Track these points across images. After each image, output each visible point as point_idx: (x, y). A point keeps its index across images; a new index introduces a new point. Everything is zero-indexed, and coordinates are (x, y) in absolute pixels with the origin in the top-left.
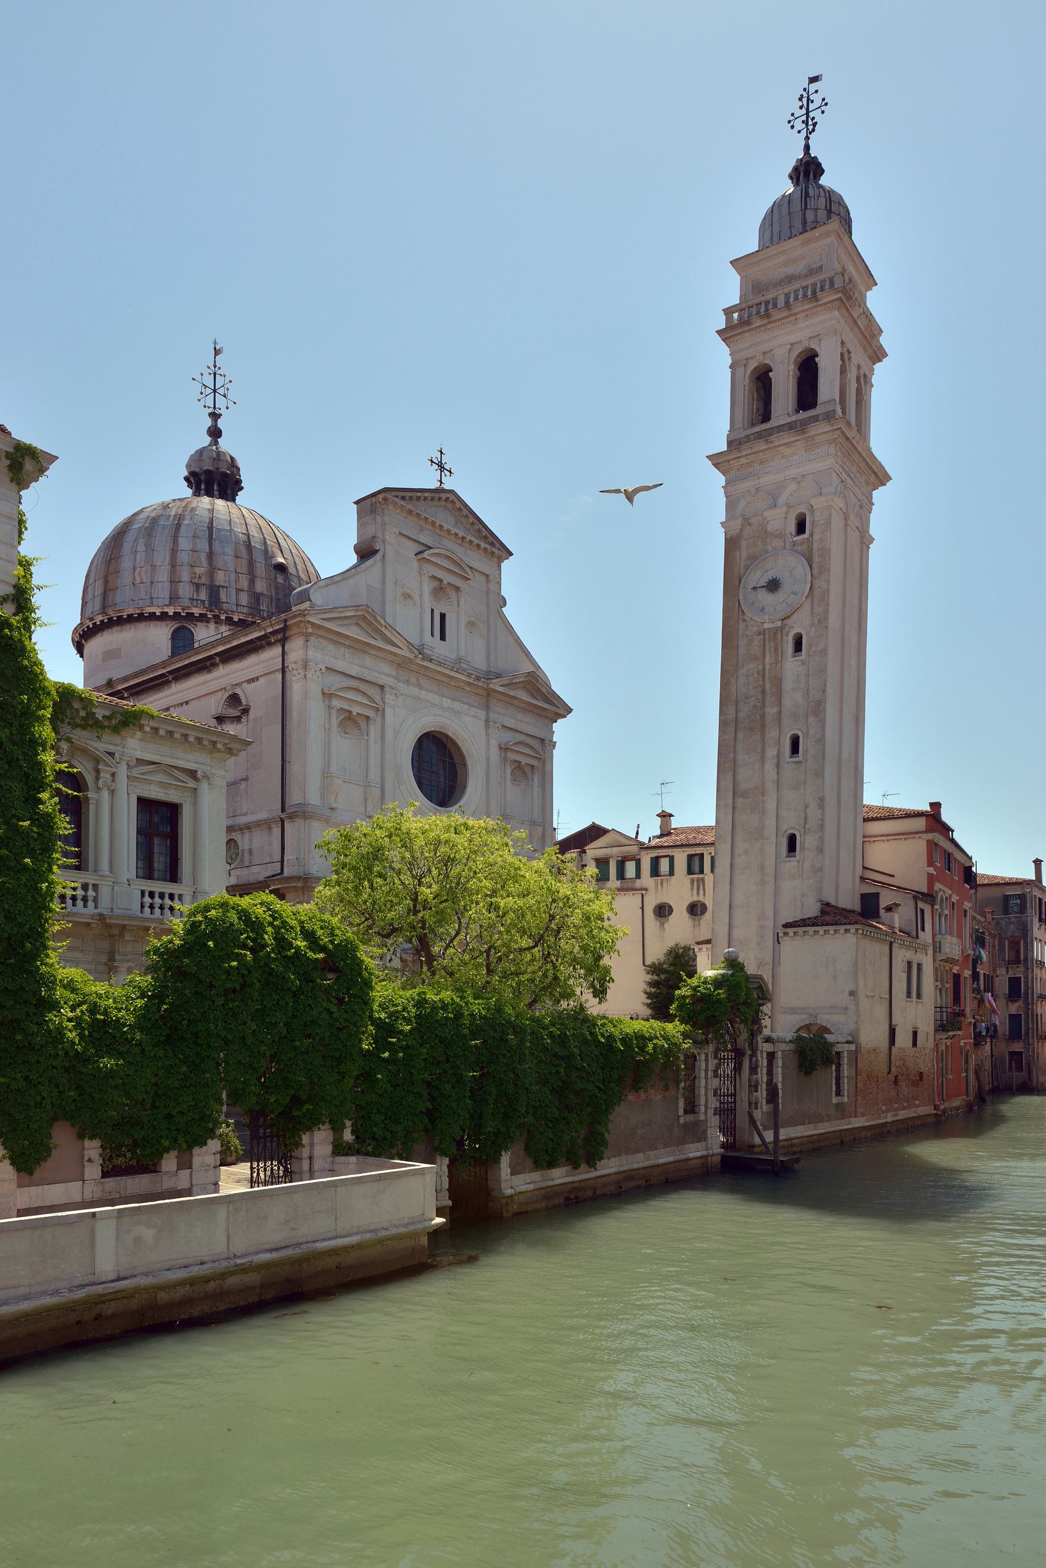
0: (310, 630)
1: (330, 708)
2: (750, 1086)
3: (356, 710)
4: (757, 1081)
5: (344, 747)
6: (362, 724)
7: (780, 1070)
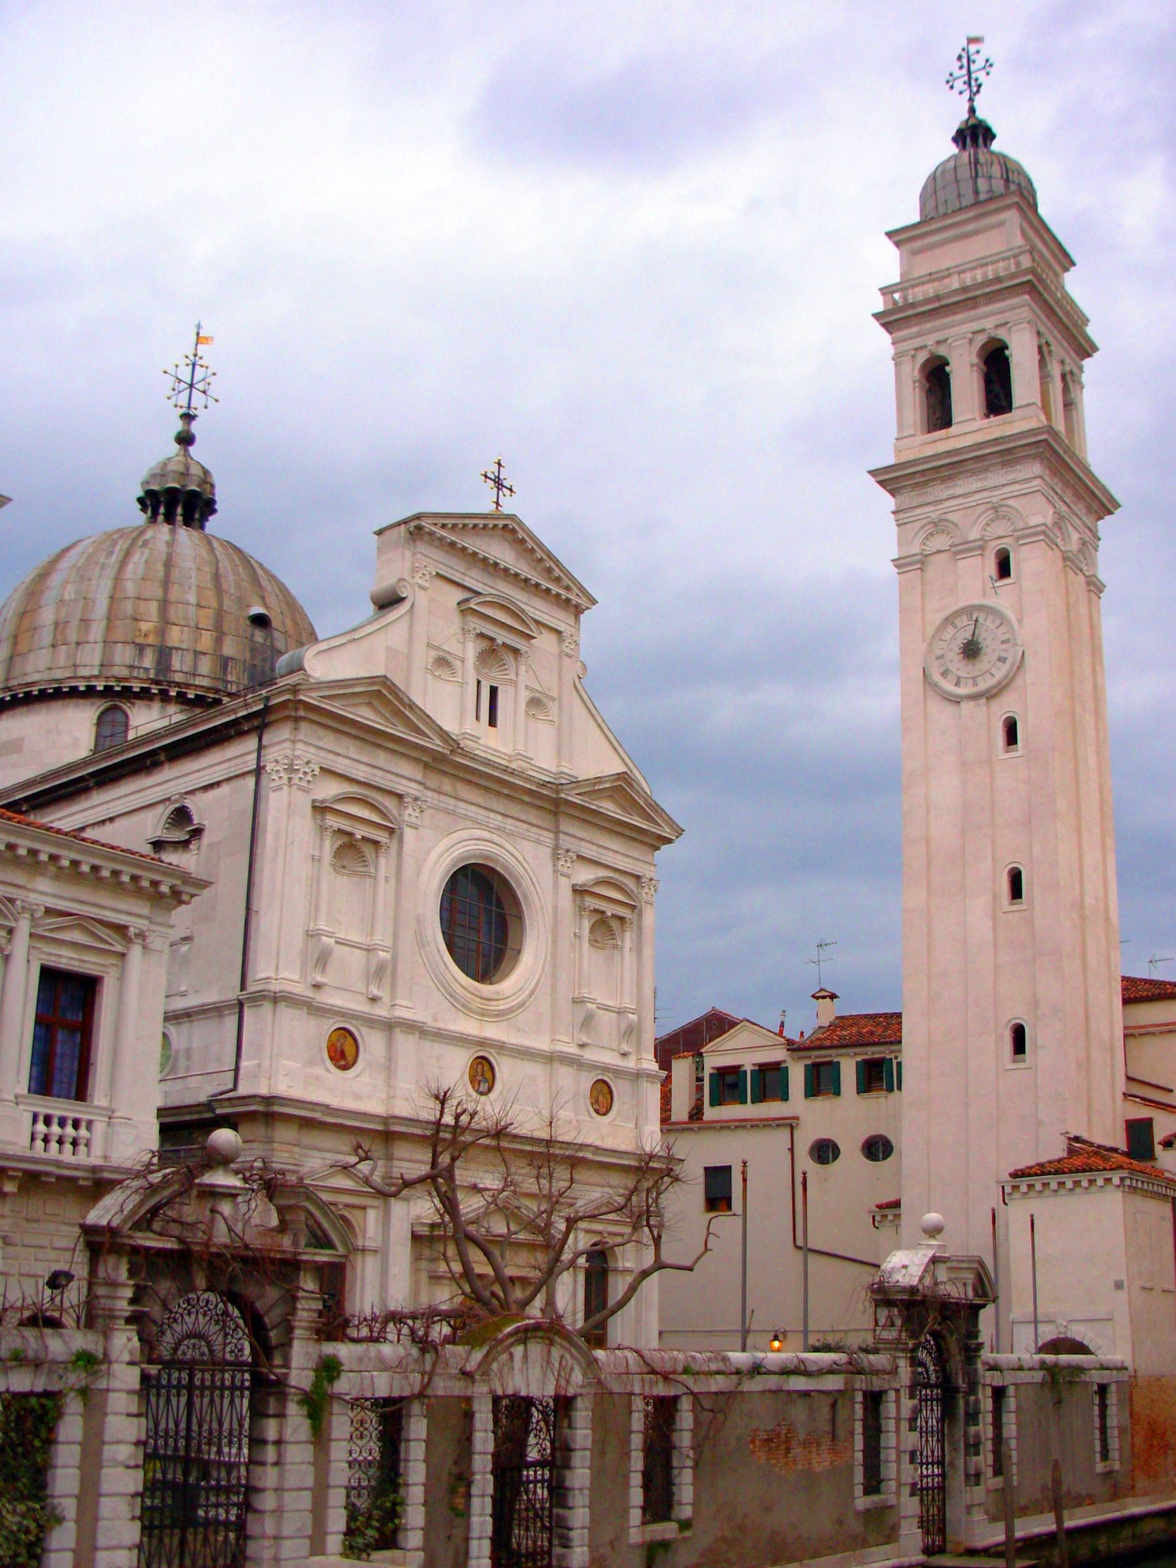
0: (302, 713)
1: (323, 829)
2: (967, 1445)
3: (360, 832)
4: (977, 1436)
5: (340, 889)
6: (368, 850)
7: (1013, 1416)
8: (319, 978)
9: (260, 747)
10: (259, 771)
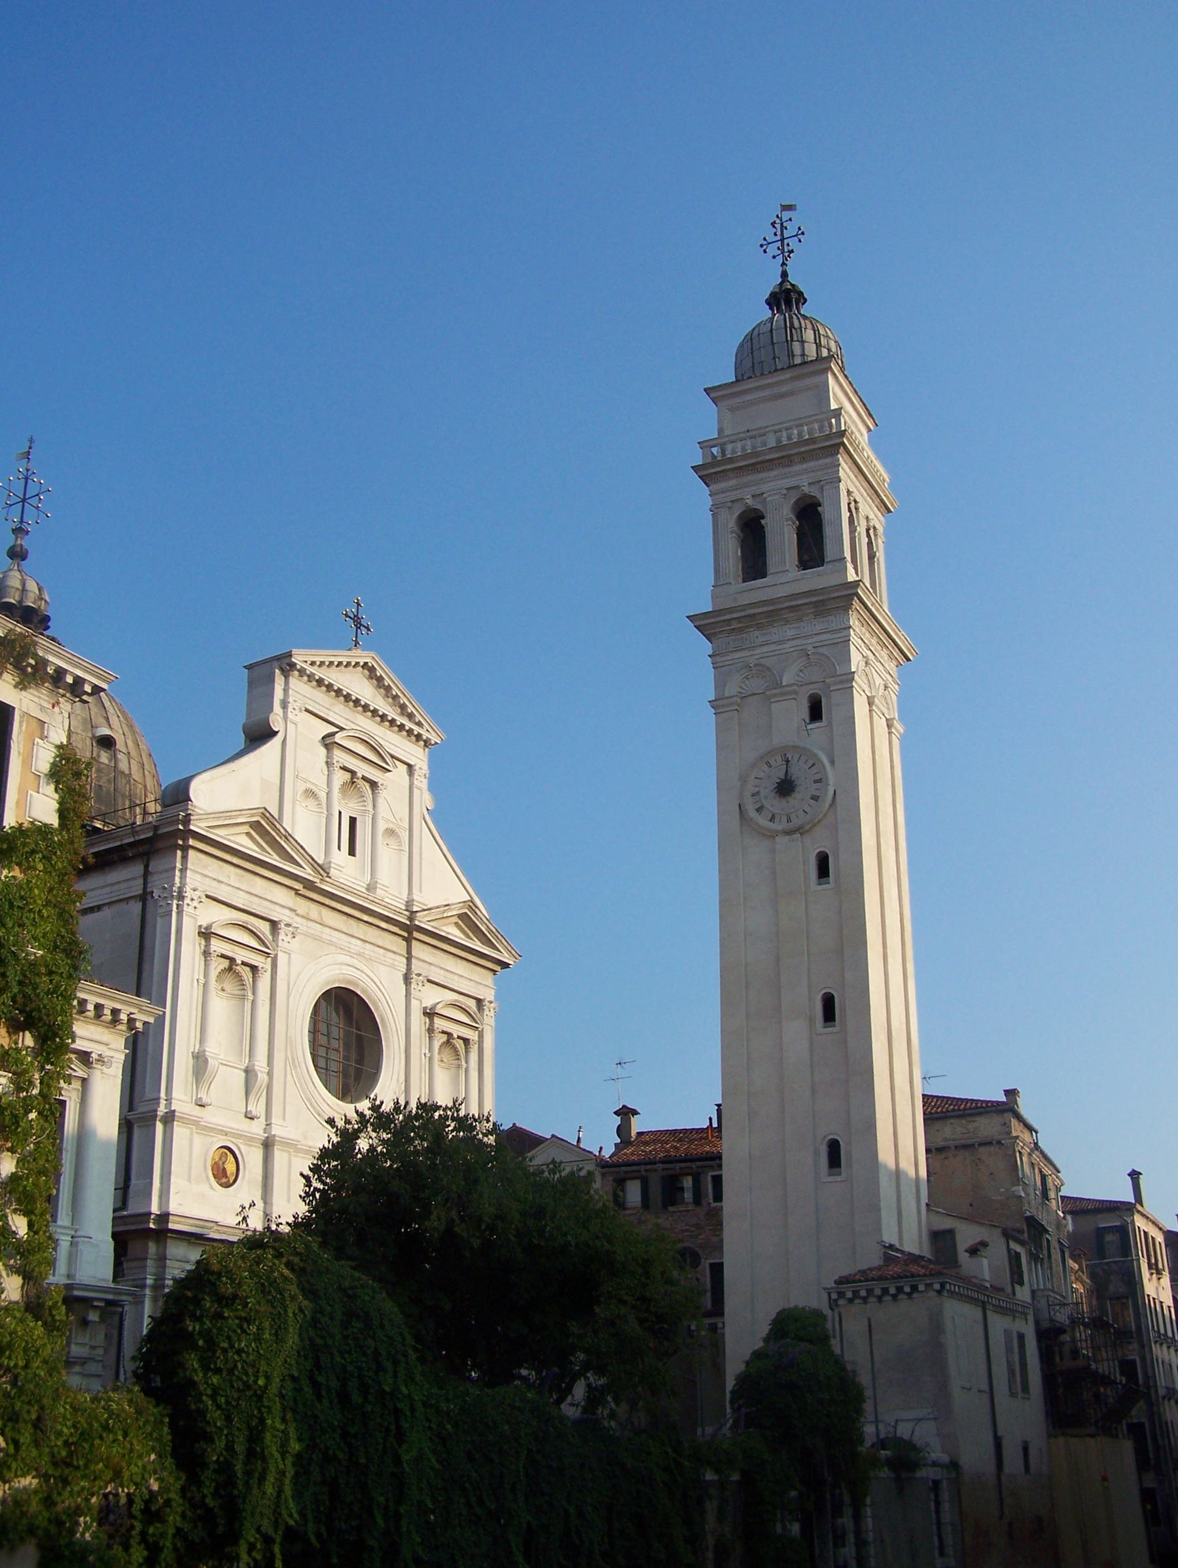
0: (191, 842)
1: (206, 953)
3: (241, 955)
6: (246, 973)
8: (205, 1100)
9: (146, 874)
10: (145, 897)
